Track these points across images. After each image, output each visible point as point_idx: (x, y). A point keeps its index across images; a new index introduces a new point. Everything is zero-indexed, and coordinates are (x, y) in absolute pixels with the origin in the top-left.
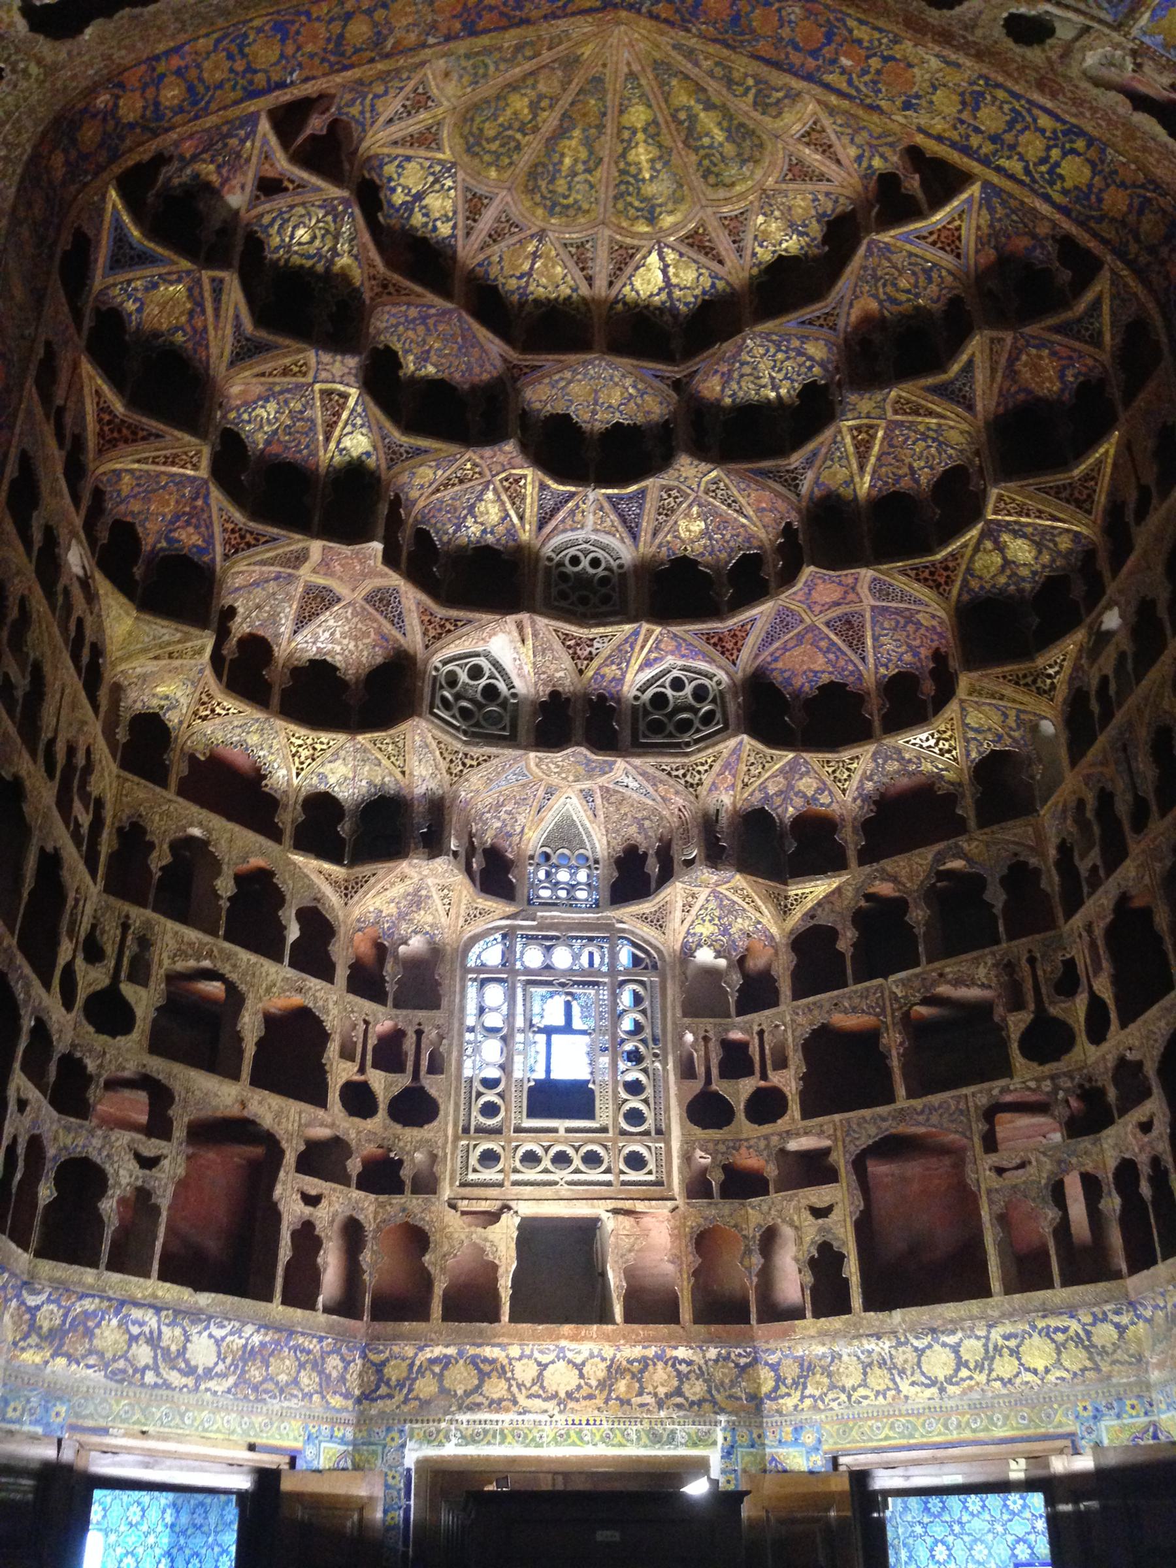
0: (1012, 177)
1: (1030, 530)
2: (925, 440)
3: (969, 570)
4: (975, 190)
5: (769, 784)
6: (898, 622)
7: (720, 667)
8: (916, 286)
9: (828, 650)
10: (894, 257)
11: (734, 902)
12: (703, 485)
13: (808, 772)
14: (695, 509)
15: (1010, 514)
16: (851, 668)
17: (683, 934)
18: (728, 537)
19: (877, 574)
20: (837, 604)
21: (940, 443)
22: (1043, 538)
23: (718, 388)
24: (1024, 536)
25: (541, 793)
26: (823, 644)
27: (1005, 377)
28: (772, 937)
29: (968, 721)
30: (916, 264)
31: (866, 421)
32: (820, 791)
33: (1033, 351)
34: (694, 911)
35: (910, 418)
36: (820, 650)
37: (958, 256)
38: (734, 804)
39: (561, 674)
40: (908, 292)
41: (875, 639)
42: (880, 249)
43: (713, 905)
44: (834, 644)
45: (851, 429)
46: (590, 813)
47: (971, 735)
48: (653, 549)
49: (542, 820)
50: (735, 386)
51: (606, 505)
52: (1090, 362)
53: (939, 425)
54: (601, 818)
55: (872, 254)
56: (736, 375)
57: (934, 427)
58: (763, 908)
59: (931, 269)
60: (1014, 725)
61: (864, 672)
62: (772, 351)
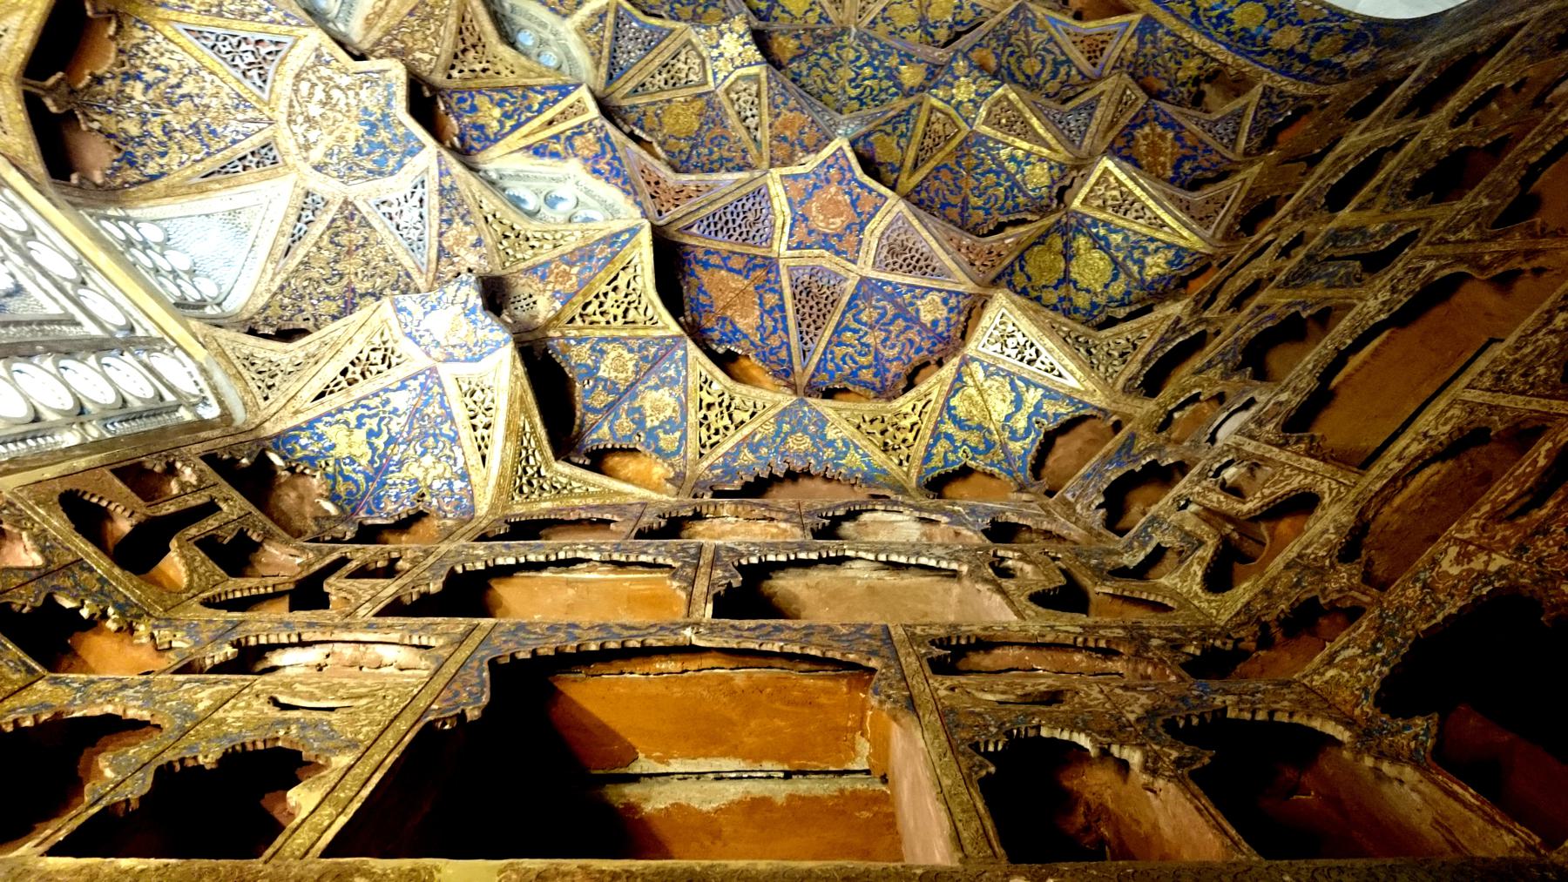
0: (1178, 17)
1: (1116, 238)
2: (998, 175)
3: (1021, 257)
4: (1136, 18)
5: (613, 351)
6: (883, 315)
7: (639, 204)
8: (1038, 75)
9: (770, 312)
10: (1033, 35)
11: (449, 417)
12: (732, 78)
13: (673, 382)
14: (699, 104)
15: (1102, 208)
16: (783, 354)
17: (300, 419)
18: (715, 156)
19: (906, 212)
20: (825, 242)
21: (1015, 184)
22: (1130, 256)
23: (789, 55)
24: (1106, 249)
25: (245, 147)
26: (771, 299)
27: (1121, 134)
28: (472, 509)
29: (954, 402)
30: (1049, 52)
31: (953, 112)
32: (669, 425)
33: (1159, 129)
34: (358, 391)
35: (999, 135)
36: (761, 305)
37: (1094, 65)
38: (548, 324)
39: (426, 57)
40: (1028, 77)
41: (838, 331)
42: (1026, 18)
43: (401, 401)
44: (782, 308)
45: (933, 109)
46: (285, 242)
47: (949, 427)
48: (626, 103)
49: (202, 191)
50: (804, 67)
51: (610, 18)
52: (1215, 158)
53: (1028, 154)
54: (293, 263)
55: (1015, 17)
56: (812, 58)
57: (1020, 154)
58: (495, 454)
59: (1062, 63)
60: (1021, 423)
61: (797, 368)
62: (863, 61)
